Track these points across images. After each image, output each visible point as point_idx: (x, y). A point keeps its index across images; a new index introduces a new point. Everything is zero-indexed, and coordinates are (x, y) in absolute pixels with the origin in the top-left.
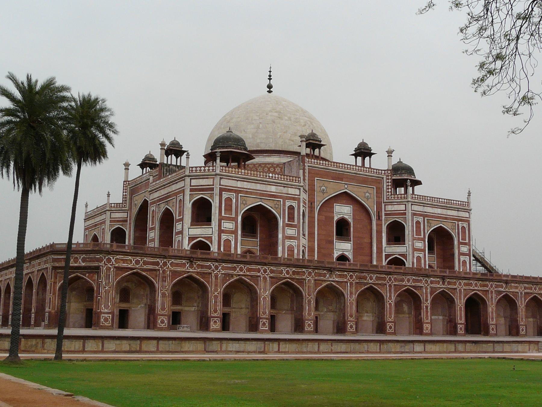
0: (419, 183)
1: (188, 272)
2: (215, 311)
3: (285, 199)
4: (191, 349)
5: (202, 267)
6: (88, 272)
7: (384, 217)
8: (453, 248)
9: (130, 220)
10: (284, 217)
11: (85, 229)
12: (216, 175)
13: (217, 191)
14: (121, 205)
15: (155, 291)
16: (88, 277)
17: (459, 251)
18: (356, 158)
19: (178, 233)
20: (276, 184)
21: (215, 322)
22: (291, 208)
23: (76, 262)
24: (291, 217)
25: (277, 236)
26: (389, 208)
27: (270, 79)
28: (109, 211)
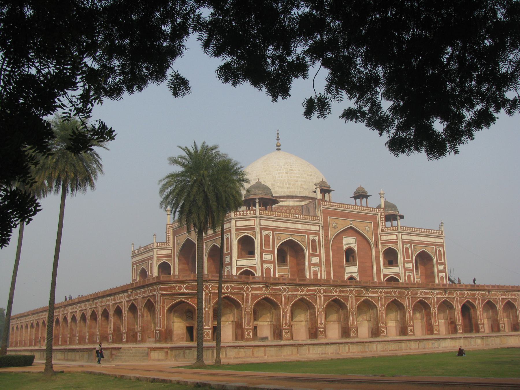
0: (402, 217)
2: (286, 324)
3: (309, 234)
5: (274, 290)
7: (380, 245)
8: (433, 267)
9: (174, 255)
10: (309, 249)
12: (256, 217)
13: (258, 230)
16: (190, 301)
17: (438, 269)
20: (302, 223)
21: (286, 333)
22: (314, 241)
23: (180, 289)
24: (314, 249)
25: (304, 264)
26: (384, 238)
27: (278, 139)
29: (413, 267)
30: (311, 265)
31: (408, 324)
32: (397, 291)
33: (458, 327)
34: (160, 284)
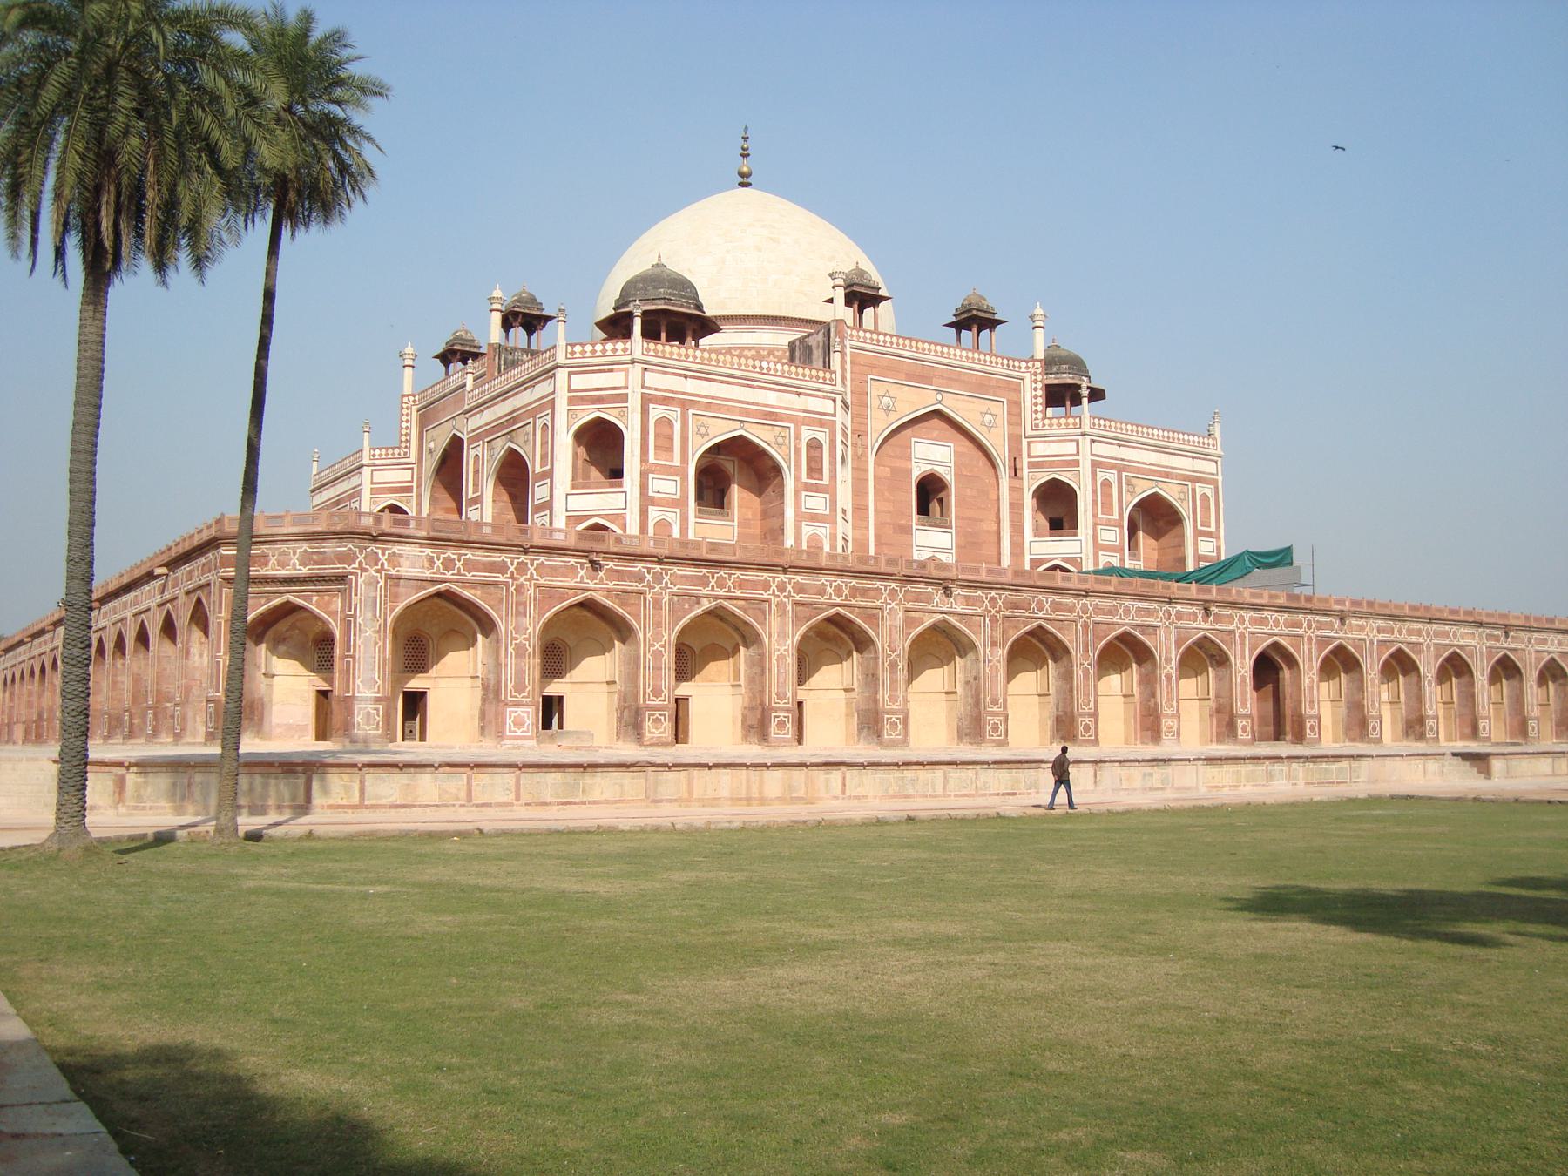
0: (1096, 395)
2: (657, 692)
3: (799, 423)
4: (607, 796)
5: (620, 575)
7: (1026, 471)
9: (419, 486)
17: (1196, 550)
19: (538, 508)
20: (779, 387)
21: (657, 720)
22: (815, 445)
23: (283, 565)
24: (815, 469)
26: (1039, 449)
29: (1122, 540)
30: (800, 517)
31: (1082, 707)
32: (1047, 600)
33: (1241, 723)
34: (218, 547)
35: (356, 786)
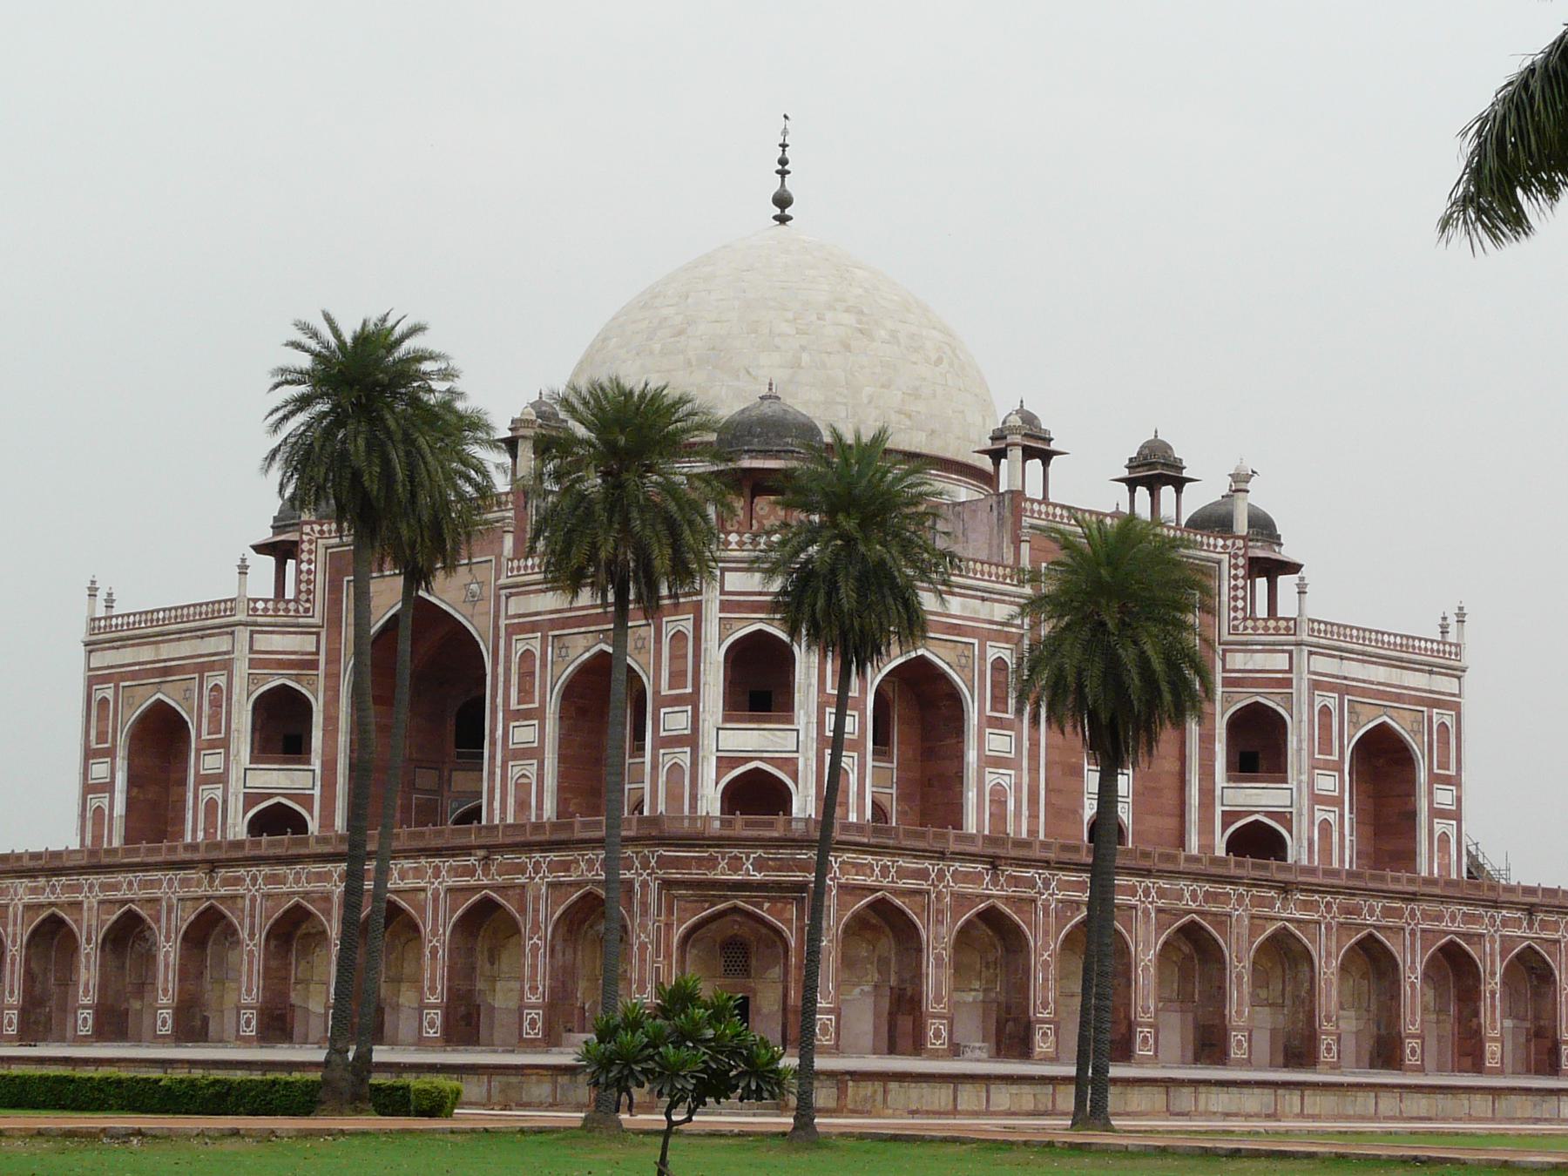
0: (1293, 568)
1: (989, 897)
2: (1045, 1006)
5: (1016, 881)
6: (769, 899)
7: (1219, 690)
9: (333, 658)
11: (94, 679)
14: (292, 606)
15: (920, 950)
16: (769, 911)
17: (1431, 802)
18: (1132, 491)
19: (677, 741)
21: (1045, 1034)
23: (736, 870)
25: (960, 756)
26: (1238, 661)
28: (246, 624)
32: (1378, 905)
35: (984, 1095)
